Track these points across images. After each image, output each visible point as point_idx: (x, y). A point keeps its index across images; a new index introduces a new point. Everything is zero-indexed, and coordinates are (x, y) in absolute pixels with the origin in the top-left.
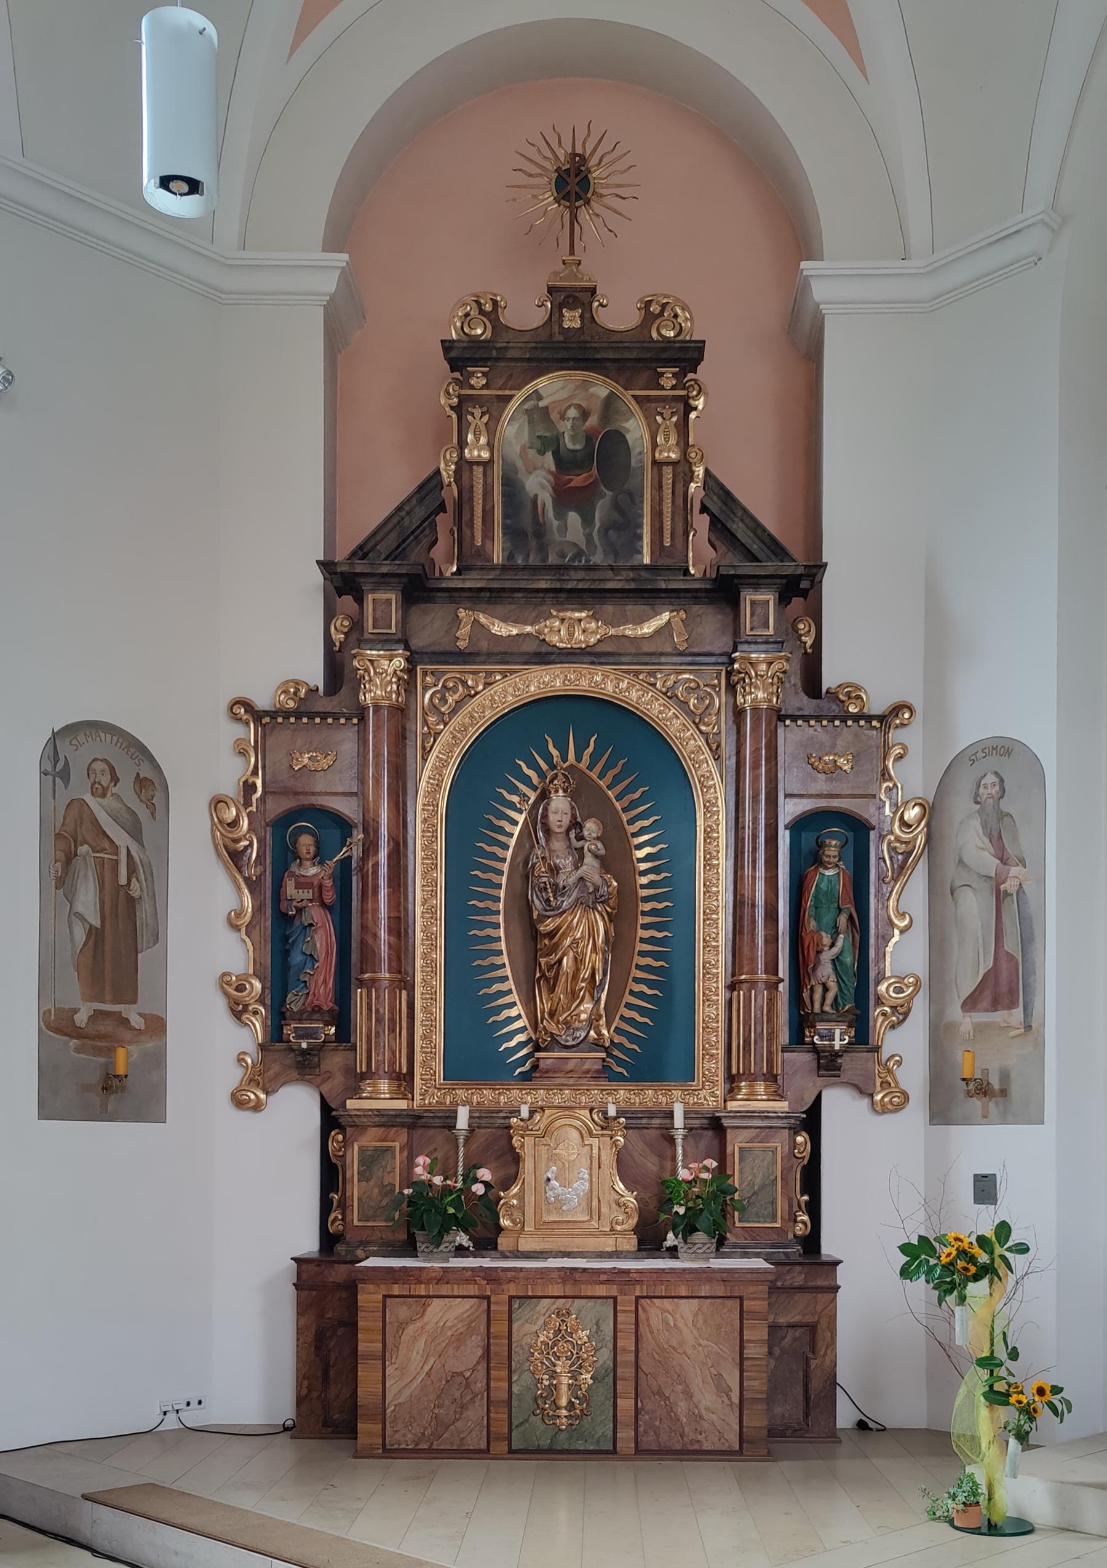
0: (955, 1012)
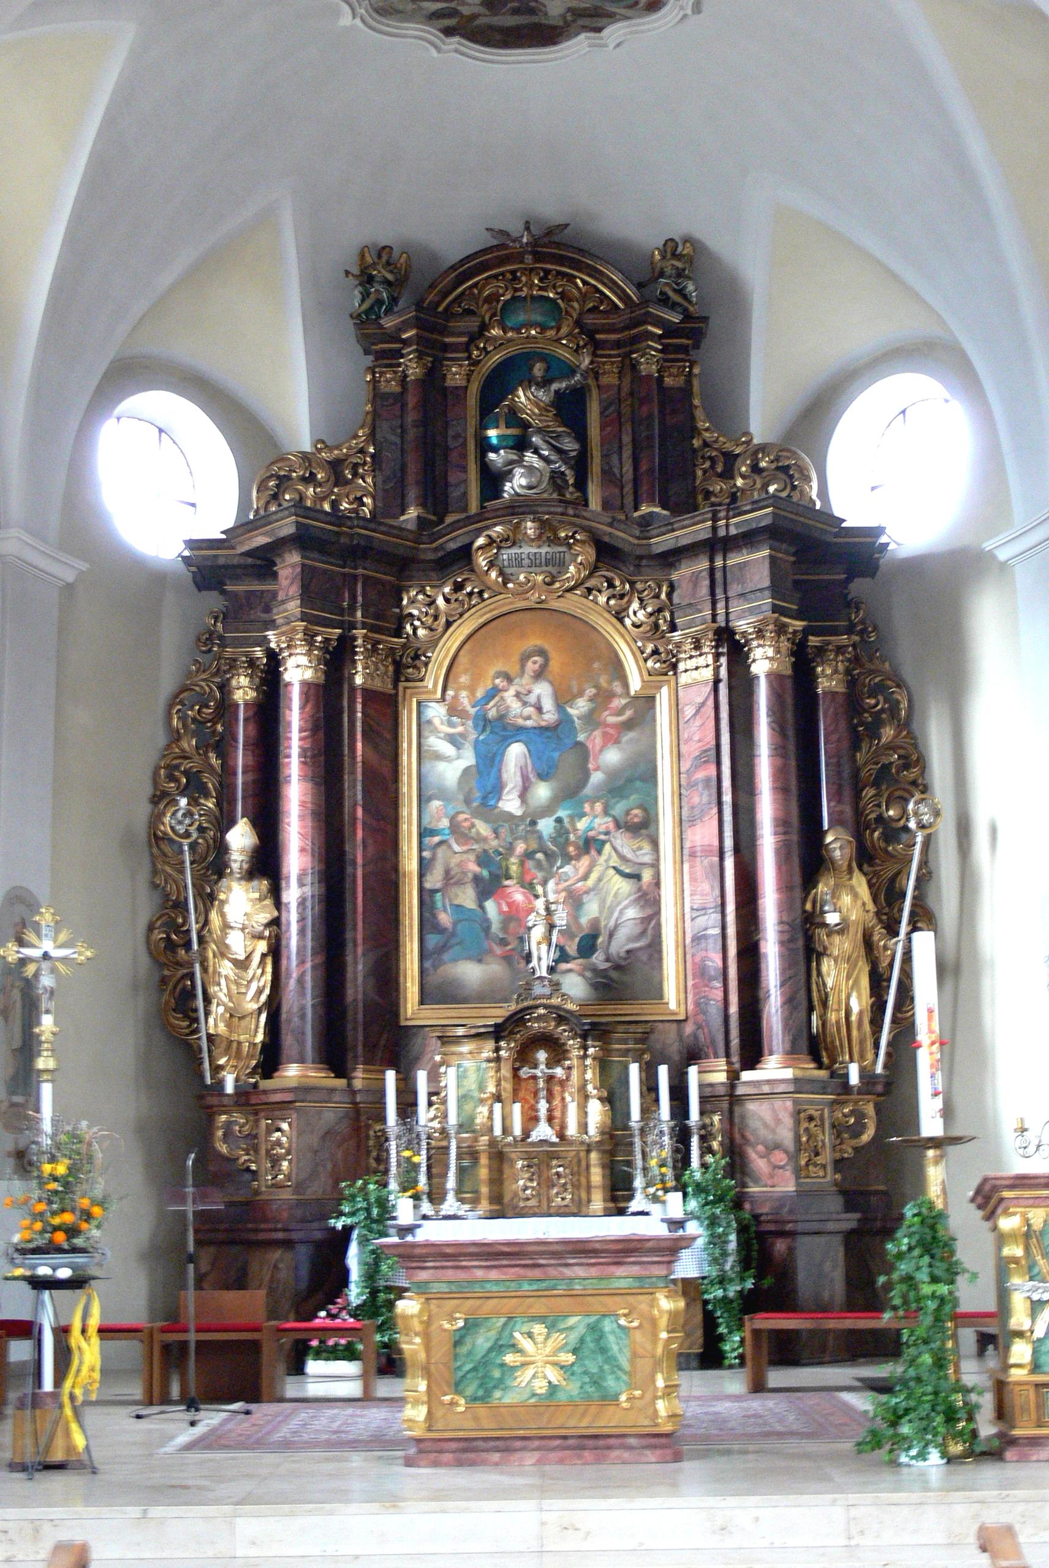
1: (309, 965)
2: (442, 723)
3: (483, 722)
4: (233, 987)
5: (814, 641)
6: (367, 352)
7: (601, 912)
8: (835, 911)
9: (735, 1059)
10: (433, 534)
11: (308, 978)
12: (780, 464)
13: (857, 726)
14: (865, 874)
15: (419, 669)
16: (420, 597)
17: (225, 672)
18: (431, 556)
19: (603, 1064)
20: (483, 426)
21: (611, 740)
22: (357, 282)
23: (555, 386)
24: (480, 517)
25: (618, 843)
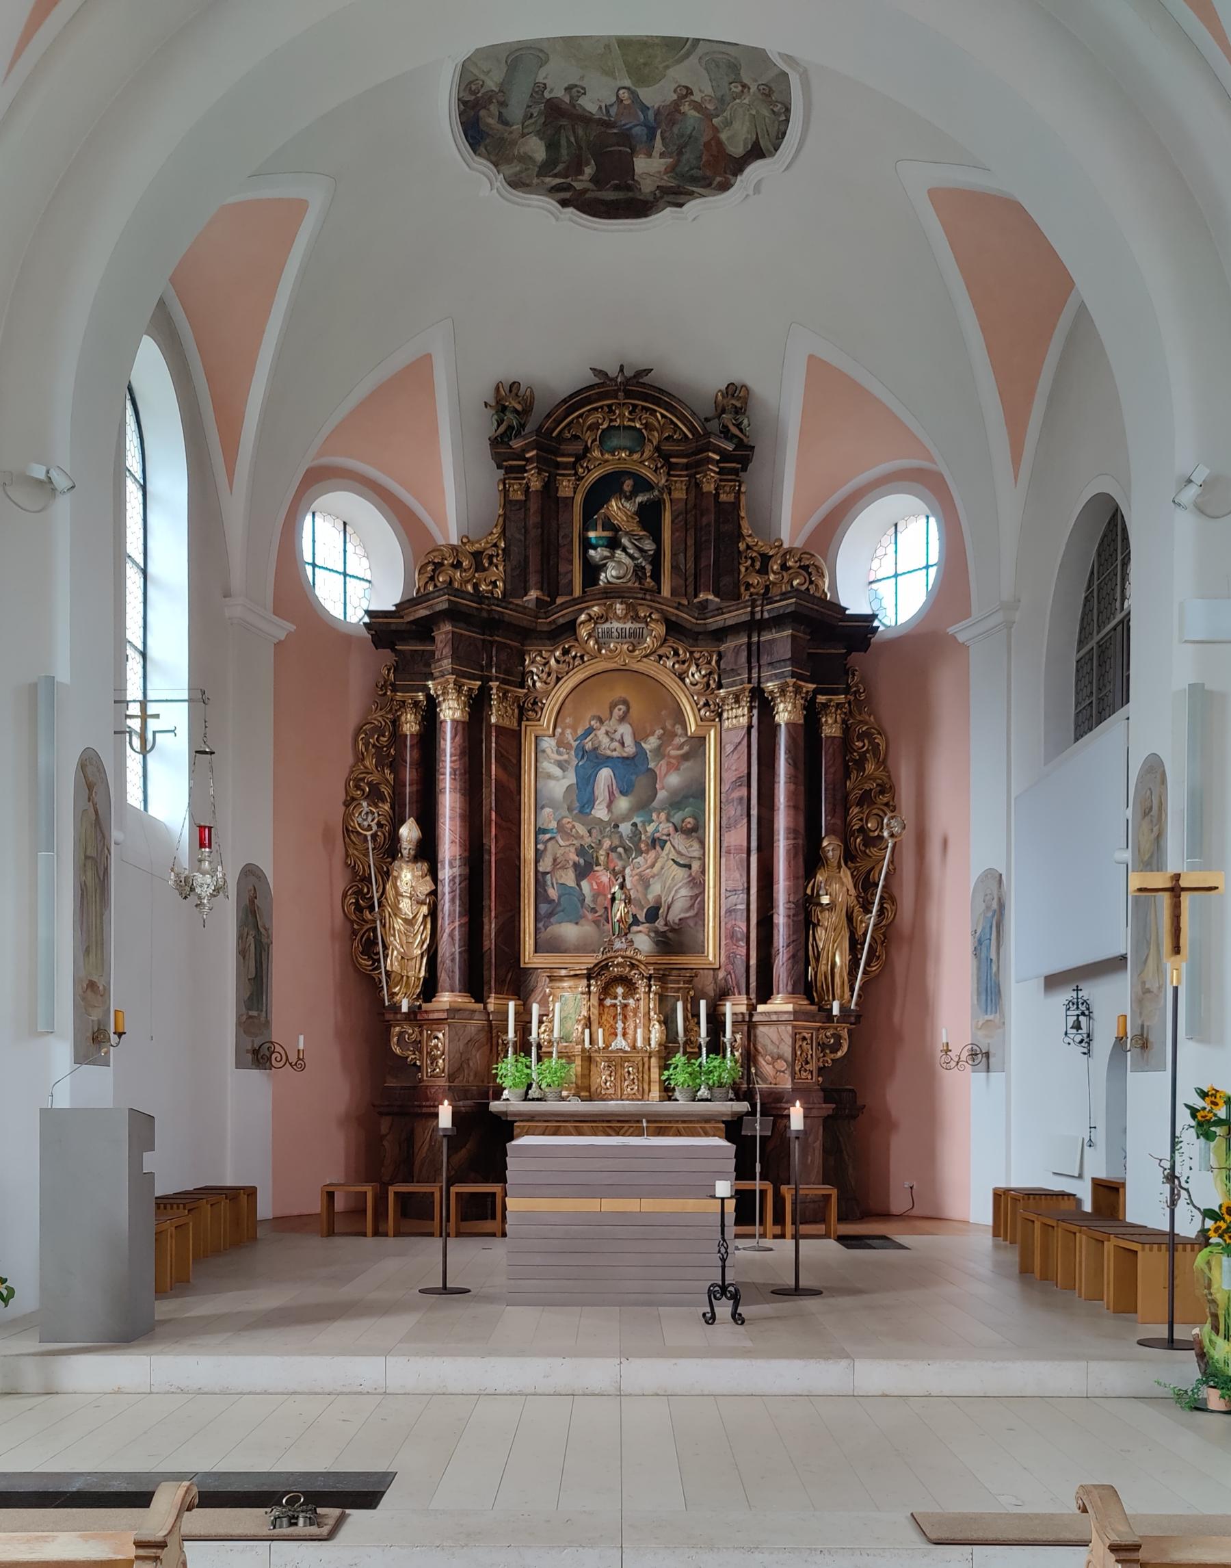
1: (457, 924)
2: (553, 752)
3: (582, 752)
4: (404, 938)
5: (821, 699)
6: (499, 467)
7: (662, 892)
8: (827, 894)
9: (753, 996)
10: (548, 611)
11: (457, 933)
12: (802, 564)
13: (849, 761)
14: (849, 869)
15: (536, 713)
16: (538, 658)
17: (396, 711)
18: (546, 628)
19: (662, 998)
20: (586, 528)
22: (494, 412)
23: (639, 499)
24: (581, 600)
25: (675, 843)
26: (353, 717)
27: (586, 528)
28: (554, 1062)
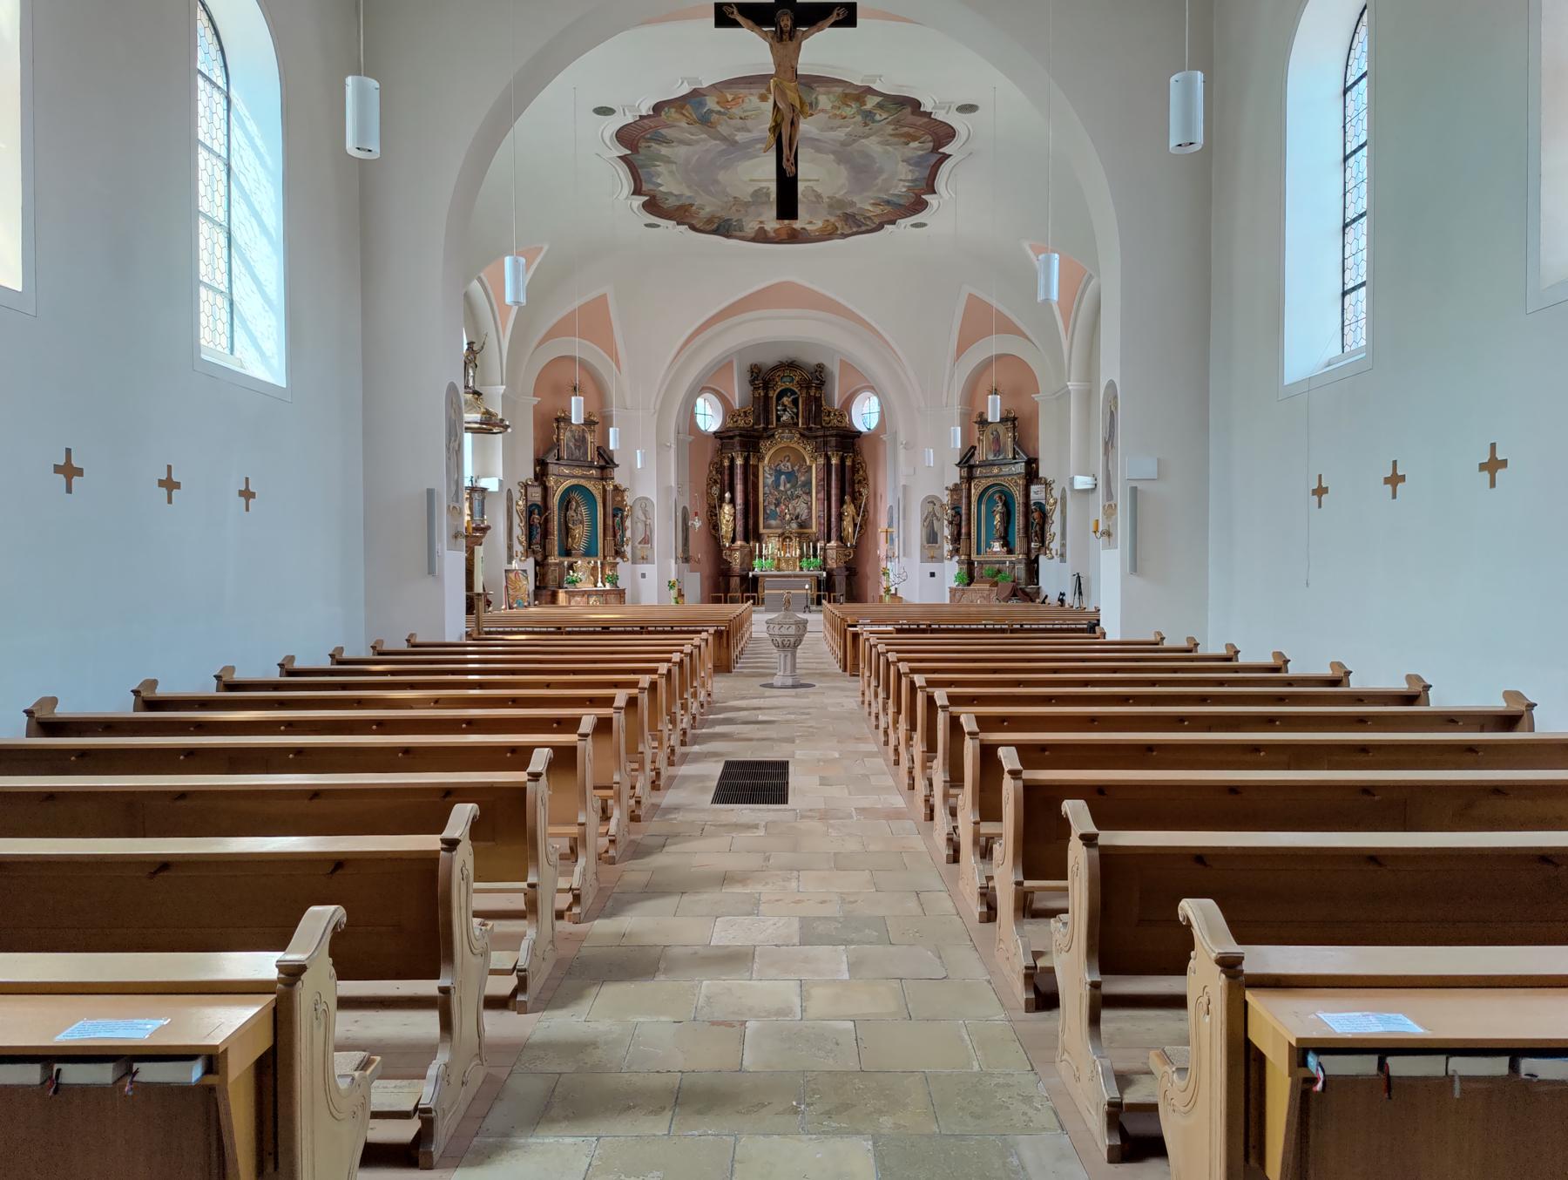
0: (637, 544)
19: (799, 542)
20: (777, 406)
21: (802, 475)
26: (709, 460)
27: (777, 406)
28: (769, 561)
